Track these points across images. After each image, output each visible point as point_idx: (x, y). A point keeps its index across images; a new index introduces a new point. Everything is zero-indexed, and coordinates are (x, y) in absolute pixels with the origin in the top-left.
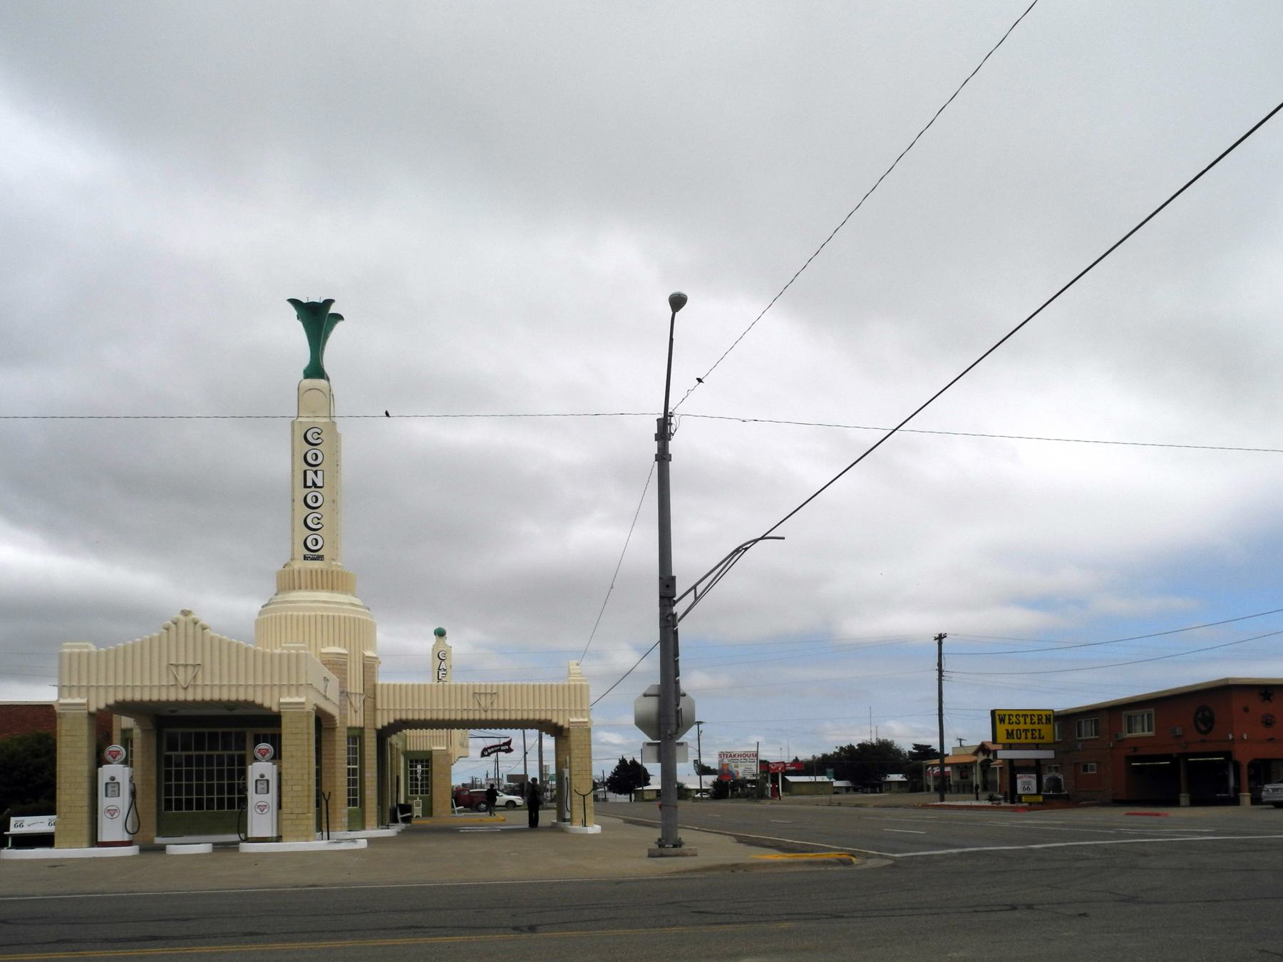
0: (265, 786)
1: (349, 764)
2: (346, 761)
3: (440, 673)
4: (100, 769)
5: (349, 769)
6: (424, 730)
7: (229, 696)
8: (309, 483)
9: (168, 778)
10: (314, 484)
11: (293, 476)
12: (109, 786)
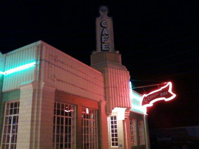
3: (103, 37)
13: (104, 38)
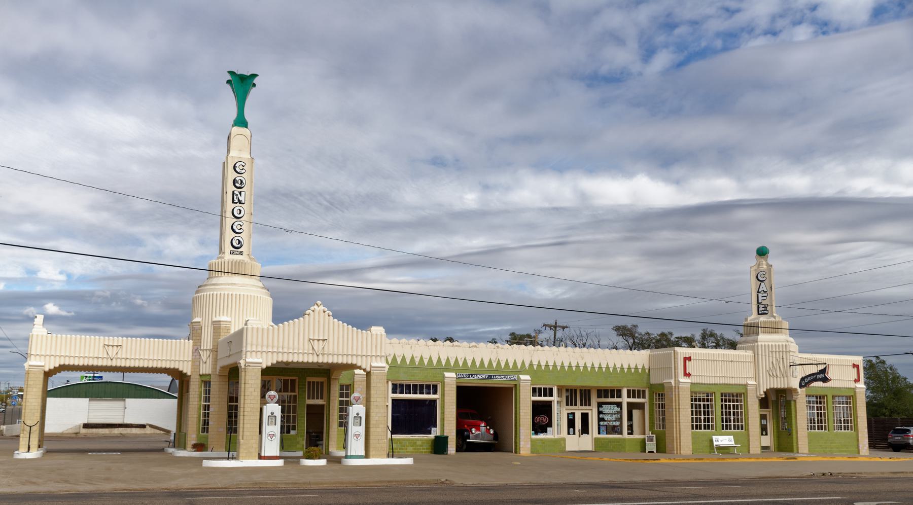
3: (760, 295)
10: (240, 202)
13: (762, 297)
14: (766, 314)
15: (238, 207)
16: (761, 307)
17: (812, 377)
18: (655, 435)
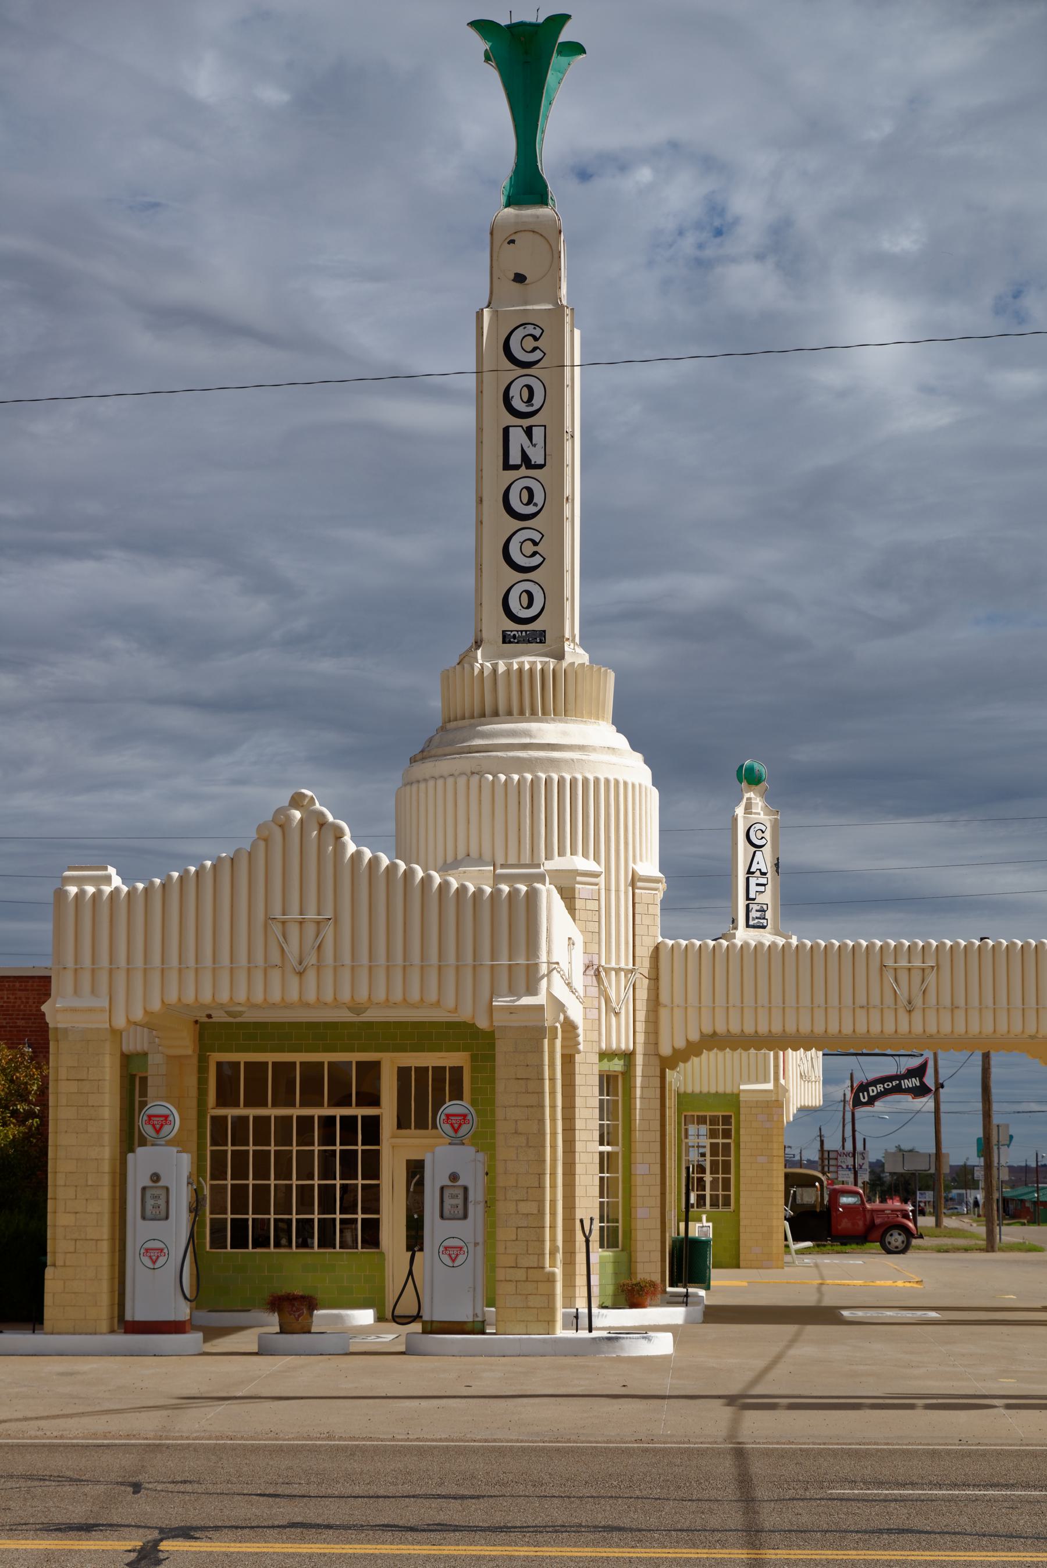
0: (459, 1201)
1: (601, 1143)
2: (596, 1136)
3: (753, 881)
4: (130, 1156)
5: (601, 1154)
6: (752, 1051)
7: (473, 1017)
8: (515, 458)
9: (218, 1172)
11: (480, 443)
12: (148, 1193)
13: (758, 885)
14: (764, 927)
15: (522, 478)
16: (754, 910)
17: (889, 1085)
18: (710, 1224)
